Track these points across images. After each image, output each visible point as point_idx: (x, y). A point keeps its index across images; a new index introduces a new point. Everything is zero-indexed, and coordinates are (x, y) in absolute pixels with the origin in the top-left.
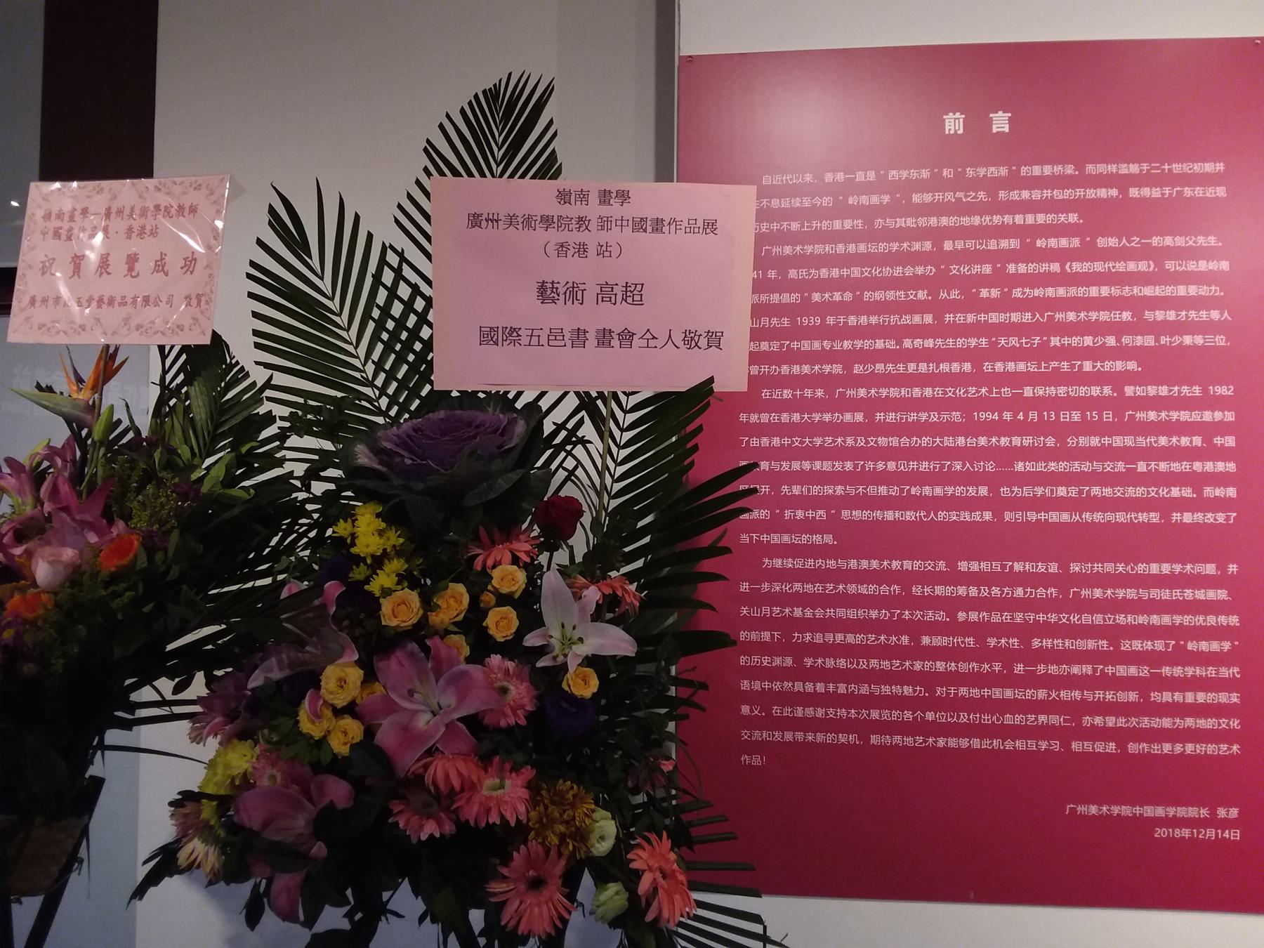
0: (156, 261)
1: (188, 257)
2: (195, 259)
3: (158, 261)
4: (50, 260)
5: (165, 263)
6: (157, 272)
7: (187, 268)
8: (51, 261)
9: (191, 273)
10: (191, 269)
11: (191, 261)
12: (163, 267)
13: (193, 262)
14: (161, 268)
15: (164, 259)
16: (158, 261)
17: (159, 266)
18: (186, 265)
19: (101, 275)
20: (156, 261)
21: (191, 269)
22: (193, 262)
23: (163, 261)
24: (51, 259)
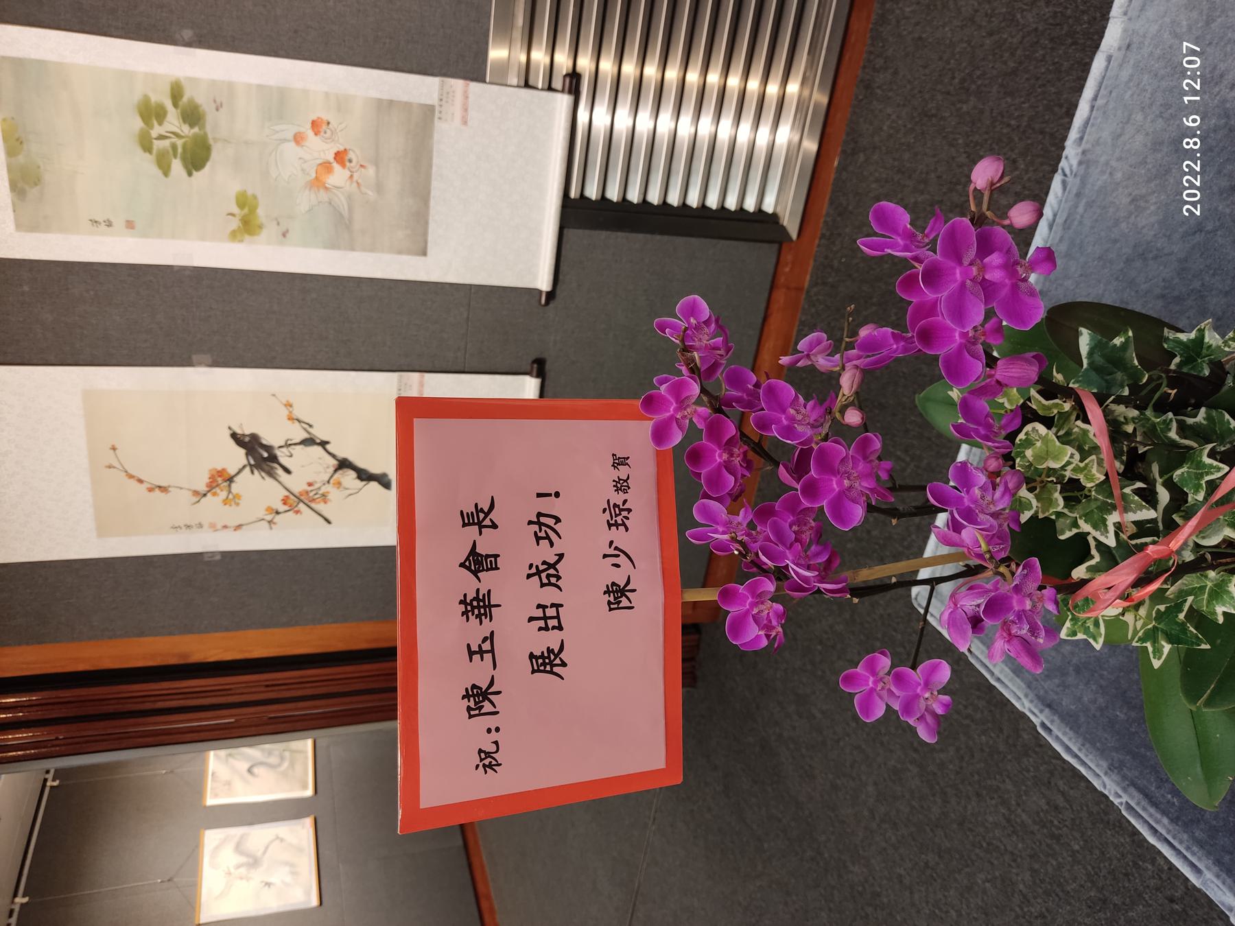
5: (544, 563)
7: (549, 531)
9: (558, 520)
10: (551, 522)
11: (540, 524)
14: (552, 571)
17: (548, 576)
20: (543, 585)
21: (551, 522)
22: (543, 519)
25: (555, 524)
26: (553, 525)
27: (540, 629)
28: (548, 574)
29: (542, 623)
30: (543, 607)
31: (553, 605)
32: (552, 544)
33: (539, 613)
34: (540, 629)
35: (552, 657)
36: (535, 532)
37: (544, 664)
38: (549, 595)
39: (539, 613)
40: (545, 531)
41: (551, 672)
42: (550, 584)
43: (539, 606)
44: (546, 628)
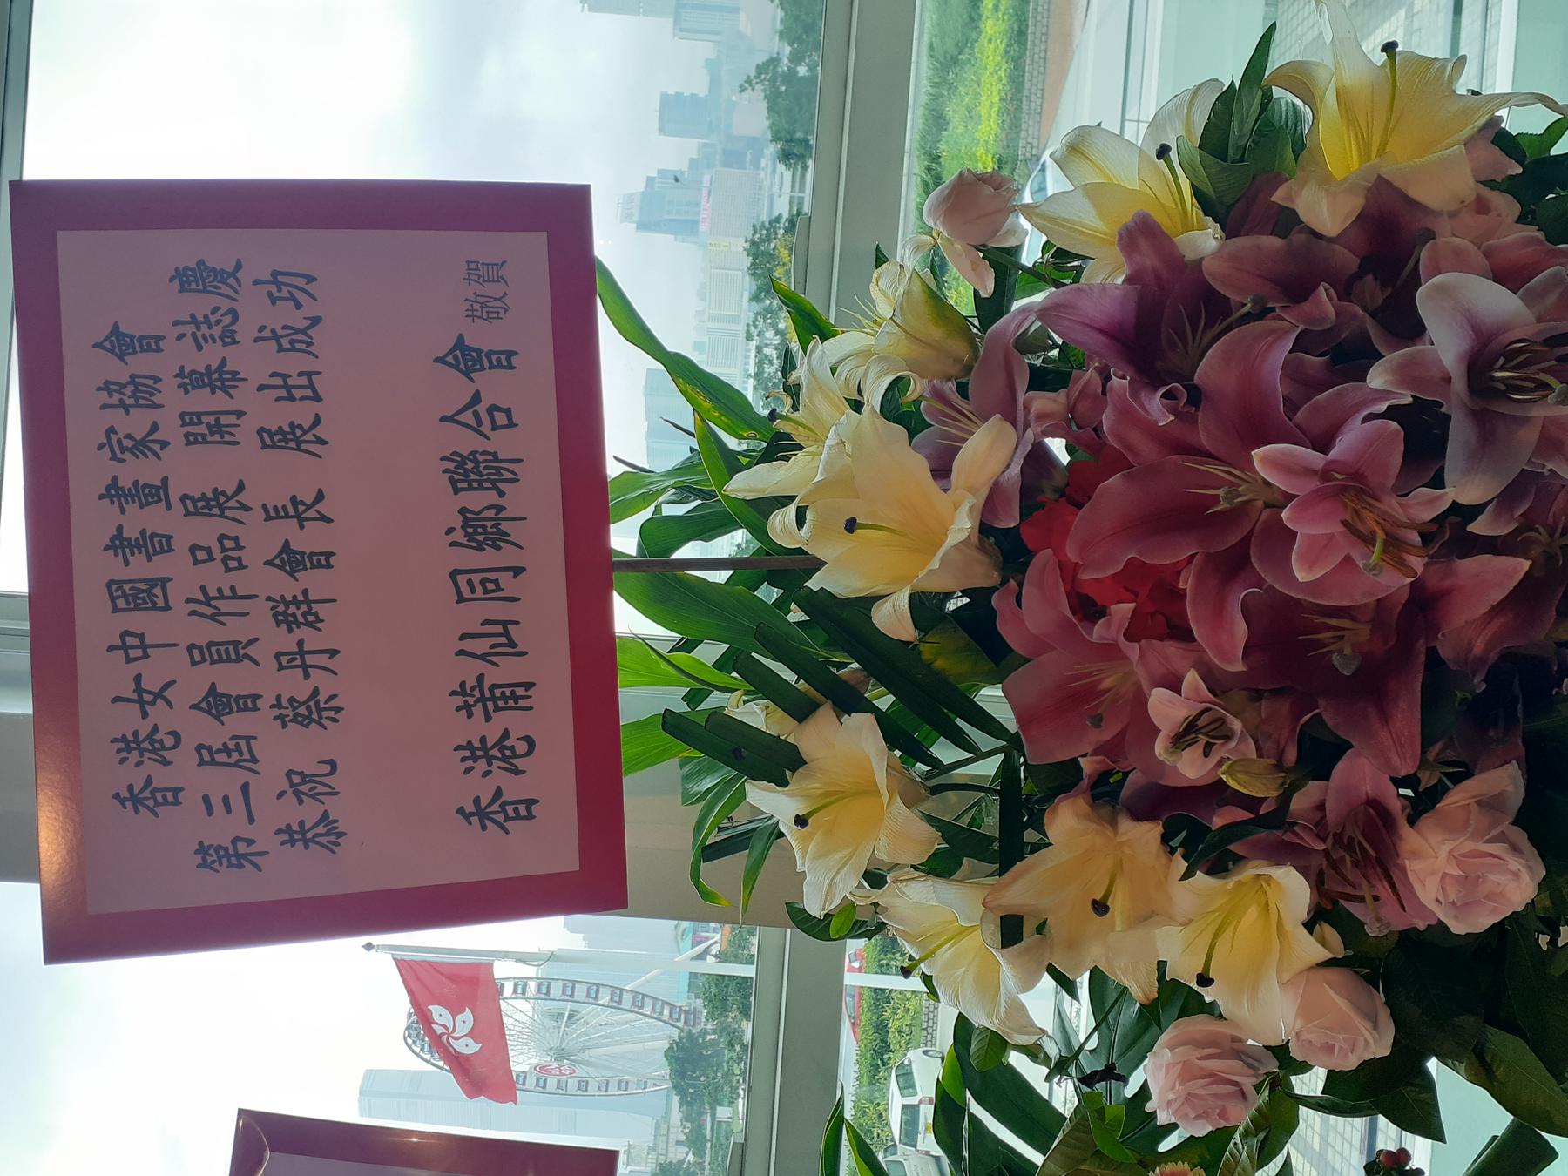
0: (281, 349)
1: (270, 294)
2: (275, 274)
3: (280, 344)
4: (292, 785)
5: (285, 327)
6: (309, 344)
7: (295, 291)
8: (296, 779)
12: (297, 331)
13: (280, 279)
15: (273, 331)
16: (280, 344)
17: (292, 342)
18: (292, 298)
19: (320, 441)
20: (281, 349)
22: (280, 279)
23: (280, 332)
24: (290, 780)
25: (307, 284)
26: (305, 287)
27: (278, 399)
28: (296, 340)
29: (283, 393)
30: (285, 377)
31: (301, 374)
32: (298, 306)
33: (278, 381)
34: (278, 399)
35: (298, 432)
36: (270, 294)
37: (287, 441)
38: (293, 364)
39: (278, 381)
40: (289, 291)
41: (298, 449)
42: (293, 349)
43: (274, 375)
44: (292, 398)
